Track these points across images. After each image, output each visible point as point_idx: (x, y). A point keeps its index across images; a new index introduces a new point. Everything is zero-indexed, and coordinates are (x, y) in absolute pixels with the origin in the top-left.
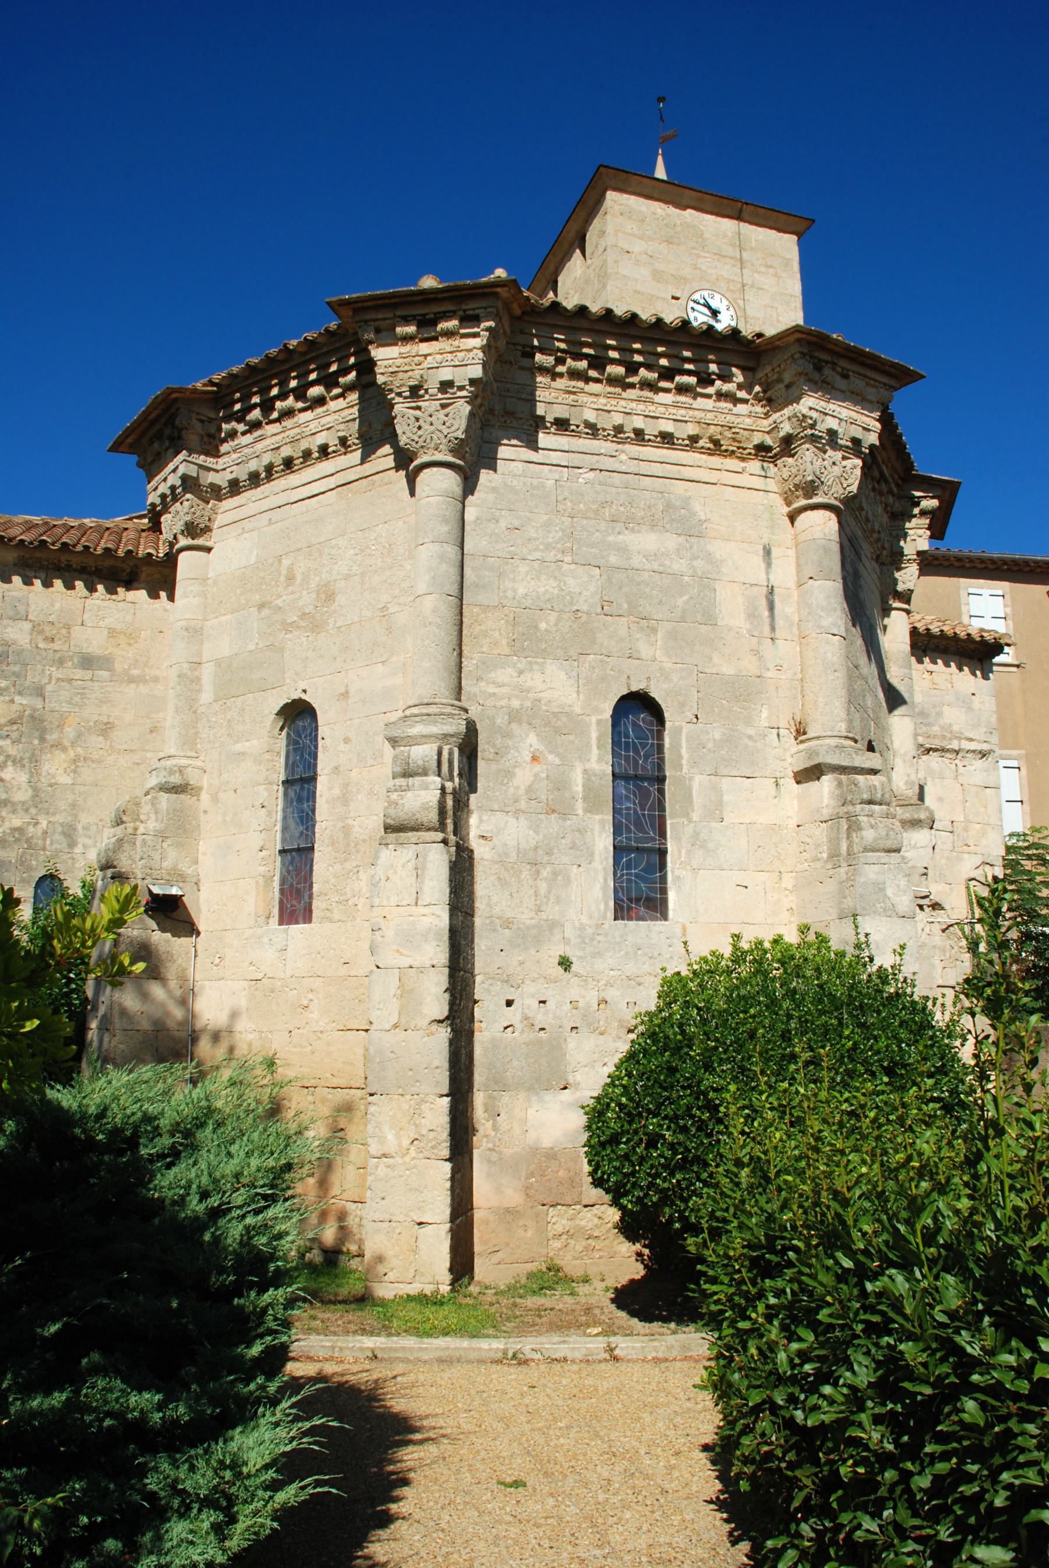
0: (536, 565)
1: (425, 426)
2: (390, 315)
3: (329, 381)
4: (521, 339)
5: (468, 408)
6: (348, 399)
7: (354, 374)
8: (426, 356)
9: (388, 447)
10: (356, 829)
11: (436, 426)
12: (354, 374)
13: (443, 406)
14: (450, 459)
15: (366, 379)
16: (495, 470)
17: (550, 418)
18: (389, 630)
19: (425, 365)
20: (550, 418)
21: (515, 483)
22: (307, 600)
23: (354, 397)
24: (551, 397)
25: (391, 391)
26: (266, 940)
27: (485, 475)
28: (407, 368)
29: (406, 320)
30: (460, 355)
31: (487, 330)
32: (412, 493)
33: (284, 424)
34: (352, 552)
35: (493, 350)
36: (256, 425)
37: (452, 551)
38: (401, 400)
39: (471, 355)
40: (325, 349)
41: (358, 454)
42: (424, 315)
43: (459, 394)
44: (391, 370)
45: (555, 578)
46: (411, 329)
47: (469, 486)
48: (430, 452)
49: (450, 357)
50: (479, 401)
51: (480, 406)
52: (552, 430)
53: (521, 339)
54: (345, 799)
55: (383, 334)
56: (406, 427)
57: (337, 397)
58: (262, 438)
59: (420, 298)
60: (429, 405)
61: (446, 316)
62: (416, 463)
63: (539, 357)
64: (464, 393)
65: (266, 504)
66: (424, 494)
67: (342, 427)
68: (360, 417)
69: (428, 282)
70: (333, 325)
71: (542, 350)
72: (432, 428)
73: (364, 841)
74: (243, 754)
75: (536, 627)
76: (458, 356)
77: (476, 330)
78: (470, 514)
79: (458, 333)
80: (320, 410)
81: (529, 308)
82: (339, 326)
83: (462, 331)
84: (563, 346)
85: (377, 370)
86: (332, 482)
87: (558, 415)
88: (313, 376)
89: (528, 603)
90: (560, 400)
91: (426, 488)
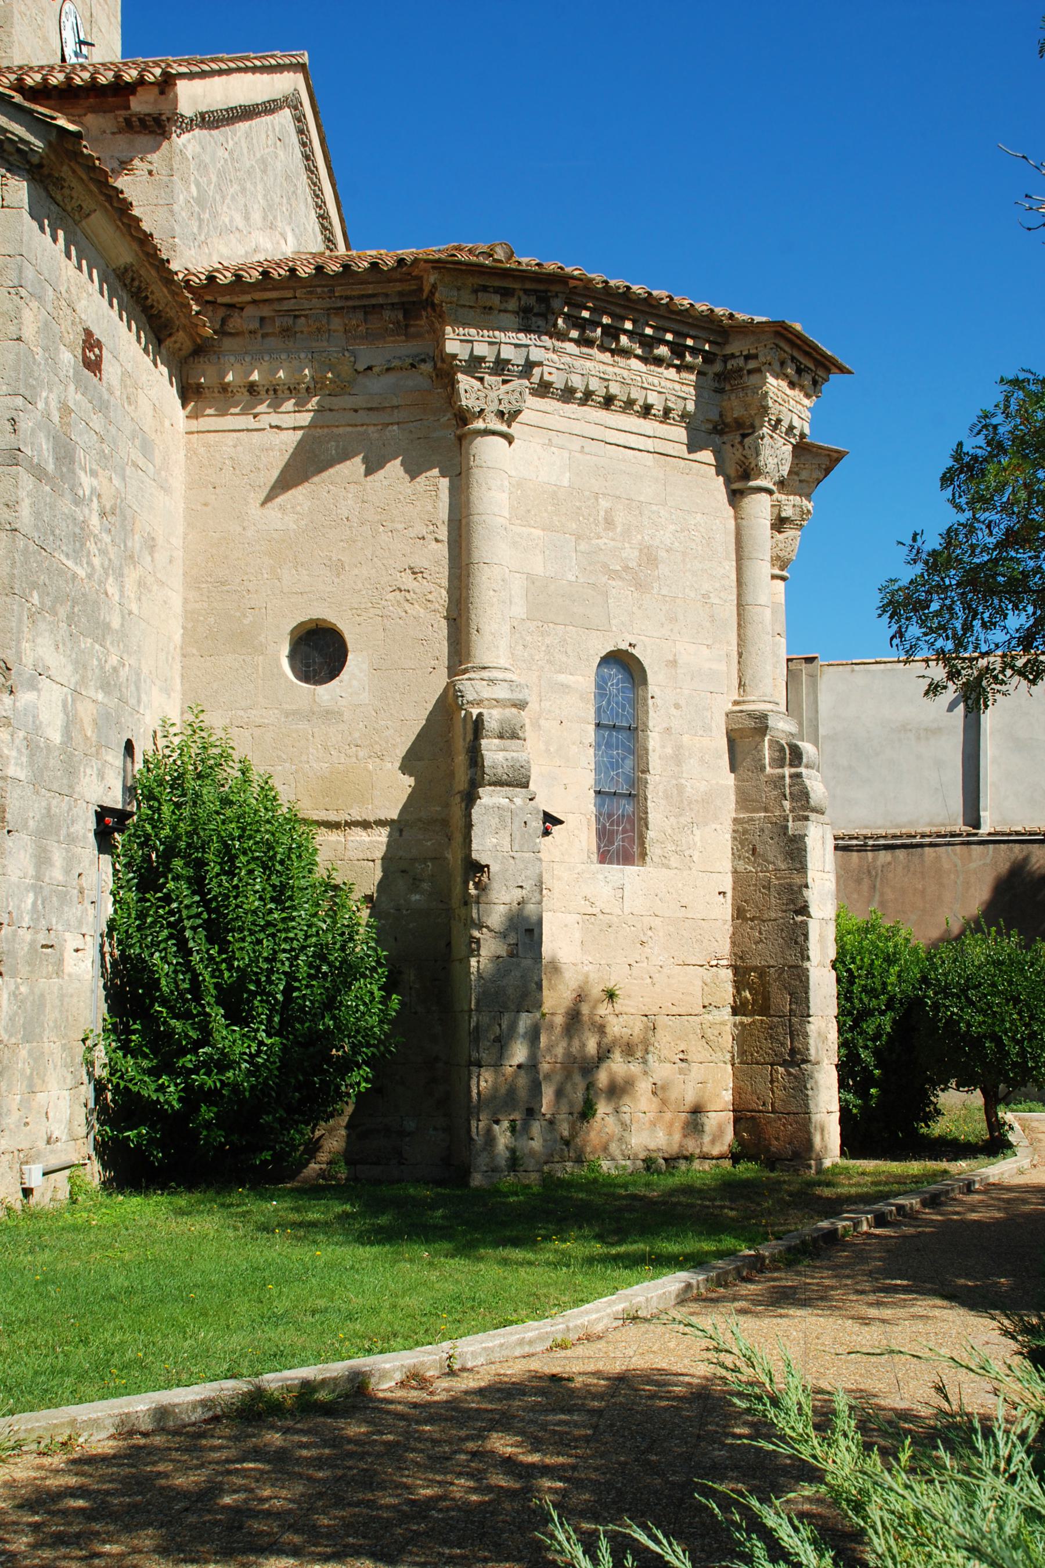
2: (787, 349)
22: (631, 554)
26: (601, 877)
33: (616, 358)
36: (589, 343)
54: (677, 758)
58: (589, 358)
65: (578, 427)
67: (673, 398)
74: (568, 687)
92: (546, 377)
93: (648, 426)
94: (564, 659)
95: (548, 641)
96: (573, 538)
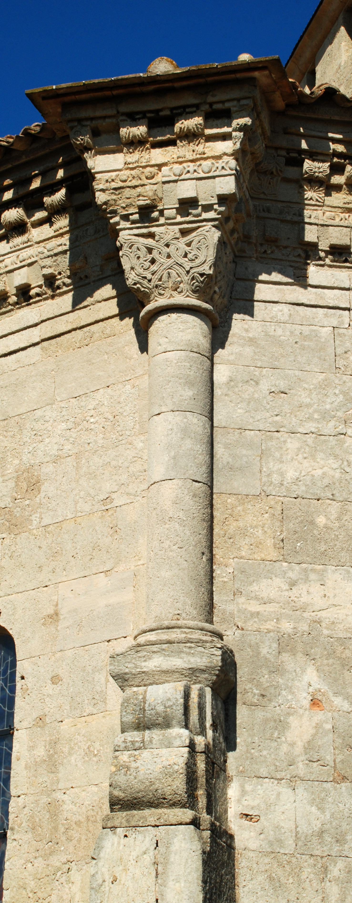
0: (310, 439)
1: (161, 259)
3: (31, 202)
4: (283, 142)
5: (217, 234)
6: (55, 227)
7: (63, 191)
8: (160, 166)
9: (109, 287)
10: (68, 806)
11: (173, 258)
12: (63, 191)
13: (184, 233)
14: (194, 301)
15: (80, 198)
16: (252, 315)
17: (324, 246)
18: (114, 529)
19: (159, 178)
20: (324, 246)
21: (279, 332)
23: (63, 222)
24: (325, 218)
25: (114, 212)
27: (239, 323)
28: (135, 183)
29: (133, 119)
30: (206, 164)
31: (241, 129)
32: (144, 347)
34: (64, 426)
35: (249, 157)
37: (197, 423)
38: (128, 225)
39: (220, 163)
40: (24, 159)
41: (69, 298)
42: (157, 111)
43: (205, 216)
44: (114, 185)
45: (336, 457)
46: (140, 130)
47: (219, 337)
48: (168, 292)
49: (192, 167)
50: (231, 224)
51: (233, 231)
52: (328, 261)
53: (283, 142)
55: (104, 137)
56: (135, 261)
57: (40, 223)
59: (151, 88)
60: (165, 232)
61: (187, 112)
62: (149, 307)
63: (308, 165)
64: (212, 215)
66: (161, 349)
67: (48, 262)
68: (71, 249)
69: (162, 67)
70: (35, 127)
71: (313, 156)
72: (170, 261)
73: (78, 823)
75: (312, 523)
76: (204, 166)
77: (226, 130)
78: (221, 374)
79: (202, 135)
80: (18, 240)
81: (295, 99)
82: (43, 128)
83: (208, 132)
84: (340, 148)
85: (97, 185)
87: (335, 241)
88: (8, 195)
89: (301, 490)
90: (337, 222)
91: (163, 341)
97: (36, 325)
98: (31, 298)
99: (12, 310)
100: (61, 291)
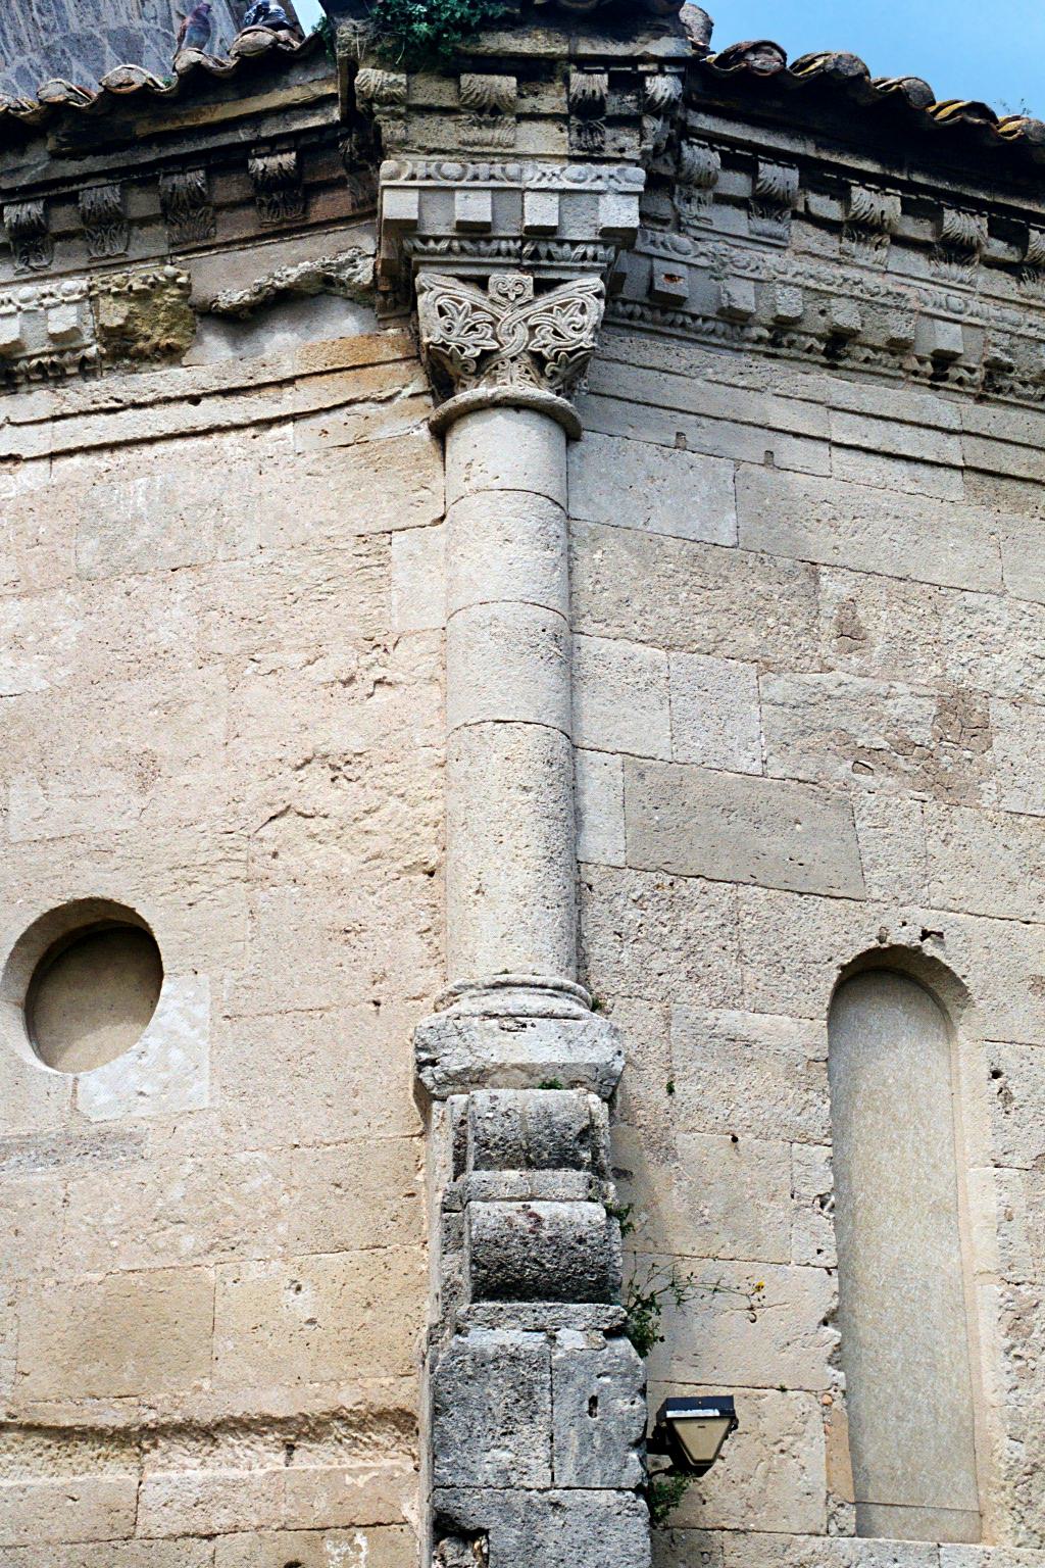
22: (911, 705)
33: (846, 244)
58: (777, 244)
86: (953, 450)
92: (661, 285)
93: (943, 408)
94: (733, 970)
95: (690, 921)
96: (752, 669)
97: (951, 432)
98: (945, 378)
99: (900, 378)
100: (1000, 397)
